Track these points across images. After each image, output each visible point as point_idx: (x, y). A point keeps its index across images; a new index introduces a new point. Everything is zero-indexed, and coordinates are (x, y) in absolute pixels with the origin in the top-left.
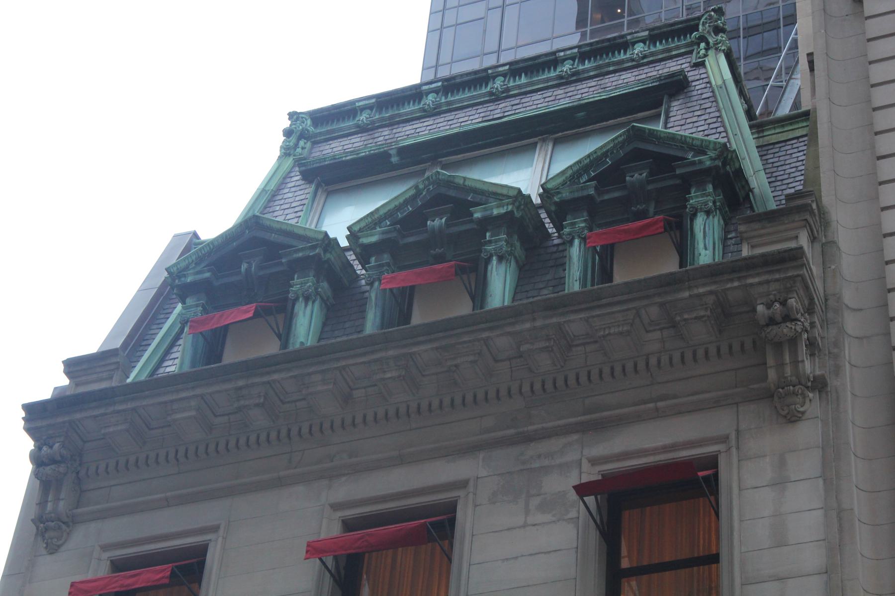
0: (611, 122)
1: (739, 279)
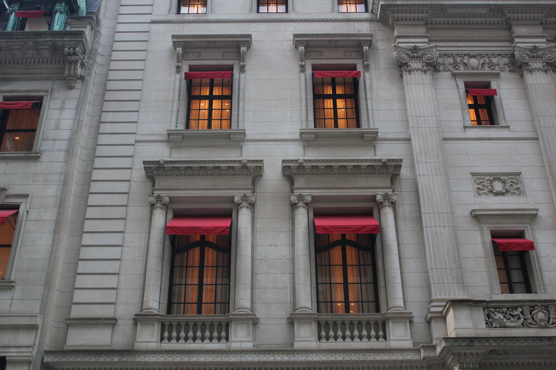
1: (61, 38)
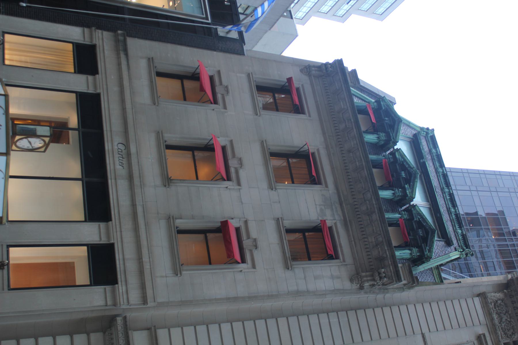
1: (392, 264)
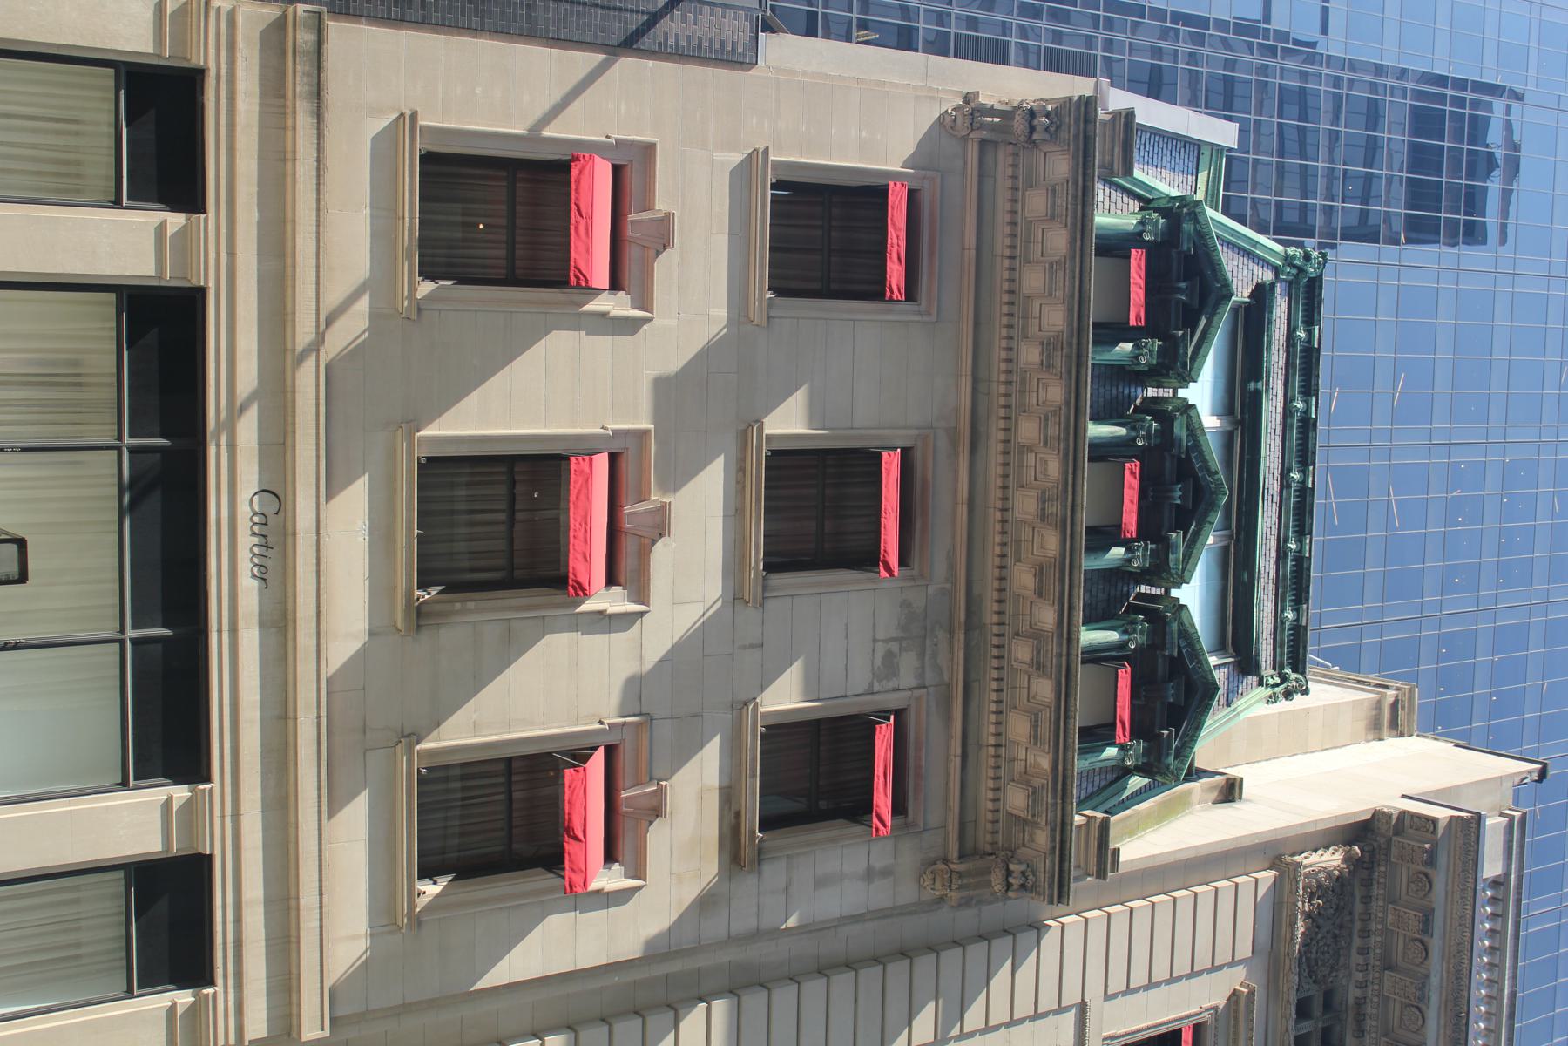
0: (1230, 628)
